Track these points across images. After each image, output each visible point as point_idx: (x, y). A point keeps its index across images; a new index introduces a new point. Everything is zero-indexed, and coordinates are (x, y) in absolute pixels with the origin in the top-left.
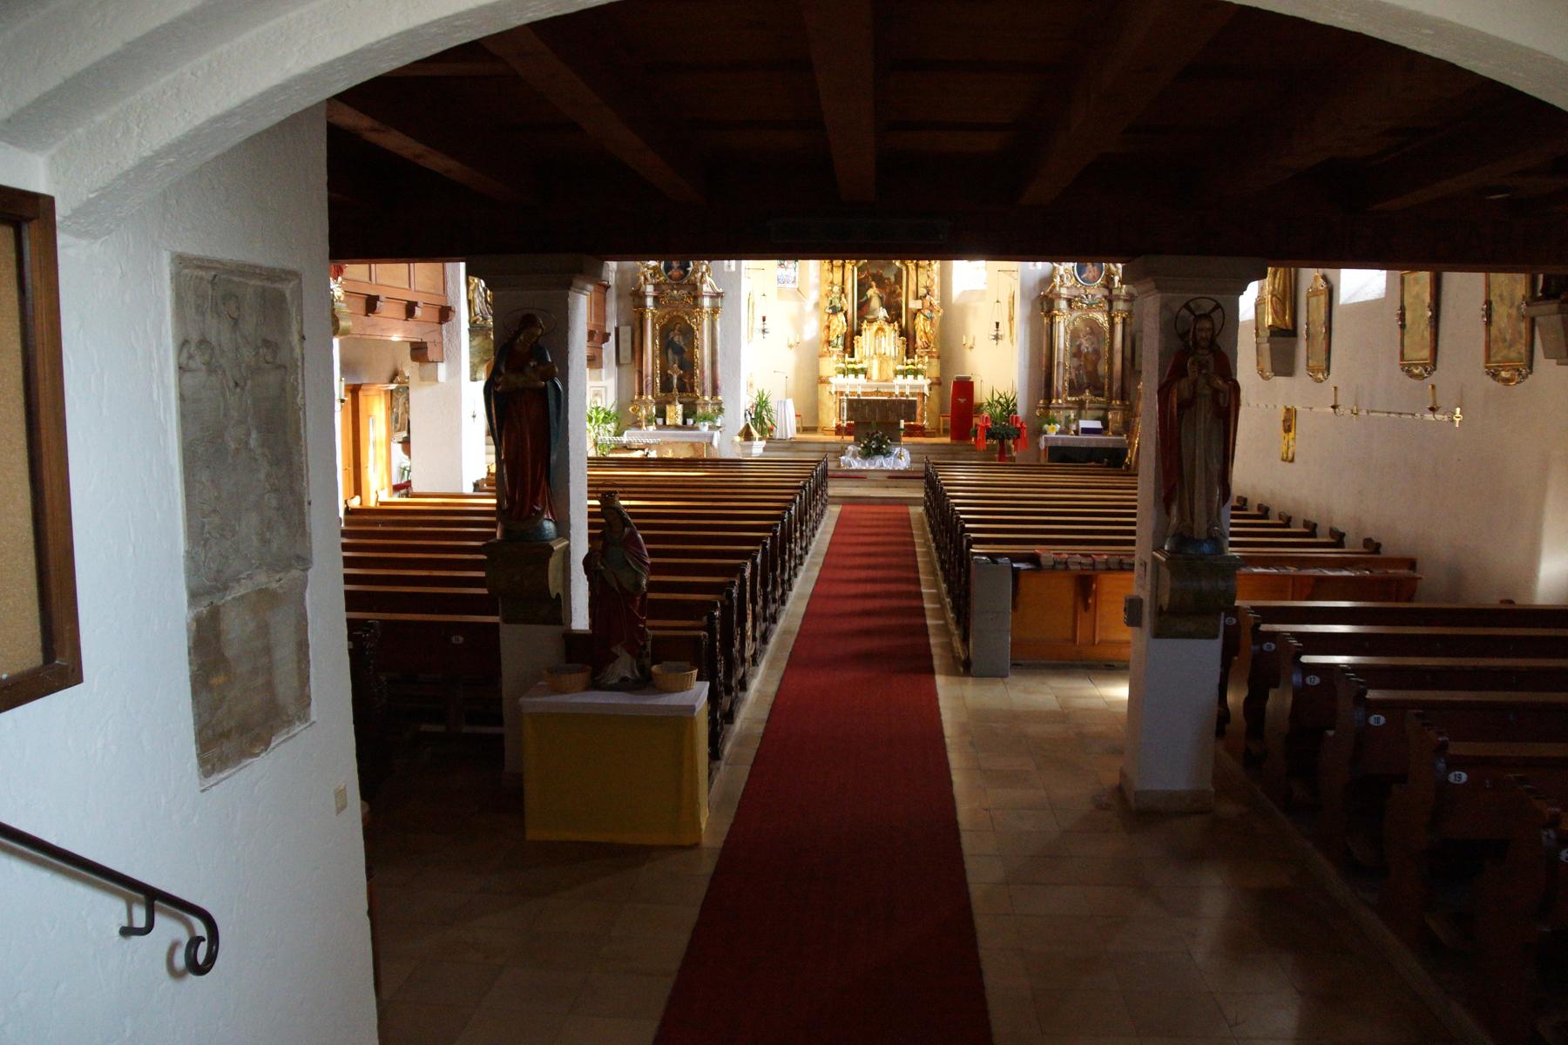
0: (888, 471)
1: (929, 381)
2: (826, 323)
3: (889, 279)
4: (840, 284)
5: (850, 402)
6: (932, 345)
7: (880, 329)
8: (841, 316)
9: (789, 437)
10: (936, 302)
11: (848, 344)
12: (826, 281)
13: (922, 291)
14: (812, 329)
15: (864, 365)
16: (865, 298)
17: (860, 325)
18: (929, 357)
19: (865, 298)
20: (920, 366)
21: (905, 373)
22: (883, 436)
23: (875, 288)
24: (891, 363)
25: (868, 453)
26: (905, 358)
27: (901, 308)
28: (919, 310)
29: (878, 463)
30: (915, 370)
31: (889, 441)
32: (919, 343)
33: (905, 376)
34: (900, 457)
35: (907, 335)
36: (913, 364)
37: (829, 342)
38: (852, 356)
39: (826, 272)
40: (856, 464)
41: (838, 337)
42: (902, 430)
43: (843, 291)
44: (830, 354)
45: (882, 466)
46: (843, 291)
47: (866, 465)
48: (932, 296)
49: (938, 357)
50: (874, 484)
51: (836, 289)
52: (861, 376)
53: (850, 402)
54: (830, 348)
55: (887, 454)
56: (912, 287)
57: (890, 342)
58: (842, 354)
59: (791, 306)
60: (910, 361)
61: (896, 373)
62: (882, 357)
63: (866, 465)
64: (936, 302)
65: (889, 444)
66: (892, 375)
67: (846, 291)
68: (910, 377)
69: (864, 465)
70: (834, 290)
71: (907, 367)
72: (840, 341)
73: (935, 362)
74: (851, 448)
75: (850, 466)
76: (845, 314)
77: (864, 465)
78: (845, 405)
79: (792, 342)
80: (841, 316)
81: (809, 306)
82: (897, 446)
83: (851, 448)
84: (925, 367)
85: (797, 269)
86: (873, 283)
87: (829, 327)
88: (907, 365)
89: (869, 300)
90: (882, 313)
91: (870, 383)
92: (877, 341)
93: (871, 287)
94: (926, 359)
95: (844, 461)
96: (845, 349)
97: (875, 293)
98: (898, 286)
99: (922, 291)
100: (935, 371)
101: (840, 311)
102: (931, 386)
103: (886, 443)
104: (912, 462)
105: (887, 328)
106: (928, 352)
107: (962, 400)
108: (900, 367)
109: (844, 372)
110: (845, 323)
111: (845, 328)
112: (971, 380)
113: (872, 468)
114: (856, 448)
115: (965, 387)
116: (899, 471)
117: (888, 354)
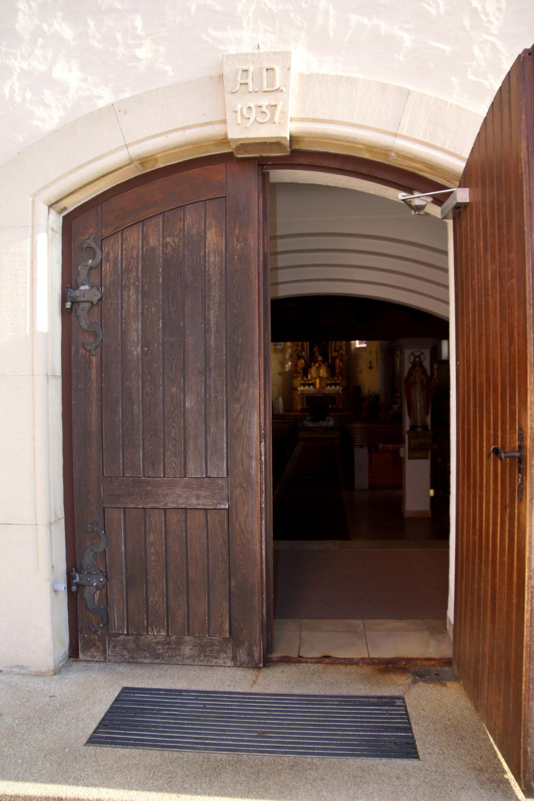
1: (341, 388)
5: (307, 397)
7: (320, 366)
10: (344, 353)
13: (338, 348)
14: (289, 365)
15: (313, 381)
17: (311, 363)
20: (338, 381)
21: (331, 385)
24: (325, 381)
25: (314, 420)
28: (336, 357)
33: (331, 386)
34: (329, 421)
35: (331, 369)
36: (335, 380)
37: (297, 372)
38: (307, 377)
40: (310, 425)
44: (297, 377)
46: (302, 349)
47: (315, 425)
51: (299, 348)
52: (311, 387)
53: (307, 397)
55: (324, 419)
57: (323, 372)
59: (280, 356)
60: (333, 379)
61: (327, 385)
62: (321, 378)
63: (315, 425)
64: (344, 353)
66: (325, 385)
68: (333, 387)
72: (302, 371)
74: (308, 418)
76: (304, 359)
78: (305, 399)
79: (280, 372)
81: (287, 357)
83: (308, 418)
87: (296, 365)
88: (332, 381)
90: (320, 358)
94: (340, 378)
99: (338, 348)
102: (343, 390)
105: (323, 365)
108: (328, 382)
109: (304, 385)
113: (317, 426)
115: (358, 389)
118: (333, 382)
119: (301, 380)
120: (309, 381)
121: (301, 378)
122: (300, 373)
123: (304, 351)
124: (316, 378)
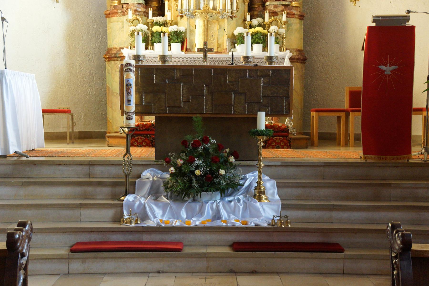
0: (233, 229)
9: (12, 152)
15: (181, 28)
18: (289, 15)
22: (219, 148)
24: (226, 23)
26: (248, 17)
29: (208, 211)
31: (232, 159)
38: (161, 11)
42: (261, 133)
45: (217, 216)
49: (301, 17)
50: (202, 264)
60: (255, 22)
65: (234, 167)
66: (226, 44)
69: (178, 216)
73: (296, 23)
75: (145, 217)
77: (178, 216)
78: (132, 77)
82: (250, 168)
88: (251, 27)
91: (189, 55)
94: (284, 17)
95: (131, 205)
103: (226, 164)
104: (284, 207)
106: (286, 6)
107: (387, 69)
112: (408, 24)
113: (196, 222)
114: (160, 173)
116: (257, 229)
117: (220, 7)
119: (132, 22)
120: (165, 24)
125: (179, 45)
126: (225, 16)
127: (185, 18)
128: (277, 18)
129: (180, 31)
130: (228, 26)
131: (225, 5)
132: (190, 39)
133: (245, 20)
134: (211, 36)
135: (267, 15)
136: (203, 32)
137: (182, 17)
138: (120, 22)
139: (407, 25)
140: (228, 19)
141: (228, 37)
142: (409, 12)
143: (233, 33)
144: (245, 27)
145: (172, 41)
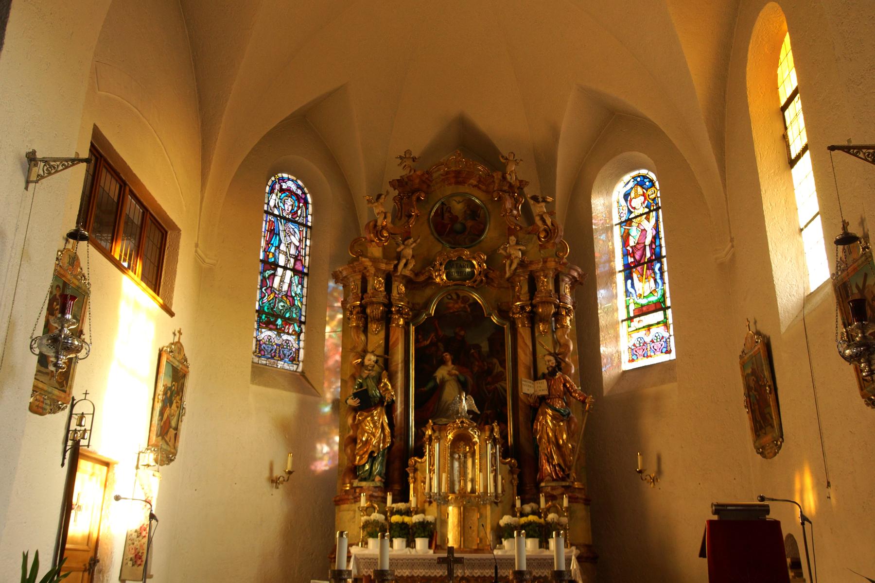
2: (351, 433)
3: (478, 347)
4: (380, 351)
6: (573, 475)
7: (462, 439)
8: (380, 416)
11: (396, 475)
12: (353, 349)
15: (430, 518)
16: (431, 385)
17: (419, 435)
18: (571, 500)
19: (431, 385)
20: (551, 516)
23: (450, 366)
26: (518, 503)
27: (505, 404)
28: (543, 401)
30: (539, 525)
32: (548, 468)
38: (403, 496)
39: (353, 334)
41: (372, 458)
43: (386, 363)
46: (386, 363)
48: (567, 371)
49: (587, 502)
51: (370, 359)
52: (421, 543)
54: (356, 483)
56: (524, 358)
58: (380, 494)
60: (527, 508)
66: (490, 537)
67: (393, 368)
70: (367, 362)
71: (524, 520)
72: (377, 467)
73: (580, 510)
76: (390, 409)
79: (278, 472)
80: (380, 416)
84: (564, 520)
85: (302, 336)
86: (448, 356)
87: (354, 440)
88: (523, 515)
89: (439, 388)
90: (465, 404)
92: (456, 464)
93: (443, 362)
96: (387, 486)
97: (449, 374)
98: (495, 361)
99: (546, 362)
100: (582, 531)
101: (376, 406)
108: (506, 520)
110: (387, 430)
111: (389, 440)
117: (479, 488)
118: (531, 518)
121: (370, 498)
122: (369, 477)
123: (391, 378)
124: (443, 501)
125: (426, 540)
126: (488, 501)
127: (434, 504)
128: (556, 503)
129: (428, 521)
130: (491, 513)
131: (486, 487)
132: (441, 532)
133: (514, 506)
134: (469, 528)
135: (542, 500)
136: (458, 523)
137: (430, 503)
138: (351, 511)
139: (767, 520)
140: (491, 505)
141: (492, 529)
142: (762, 499)
143: (498, 523)
144: (514, 515)
145: (417, 535)
